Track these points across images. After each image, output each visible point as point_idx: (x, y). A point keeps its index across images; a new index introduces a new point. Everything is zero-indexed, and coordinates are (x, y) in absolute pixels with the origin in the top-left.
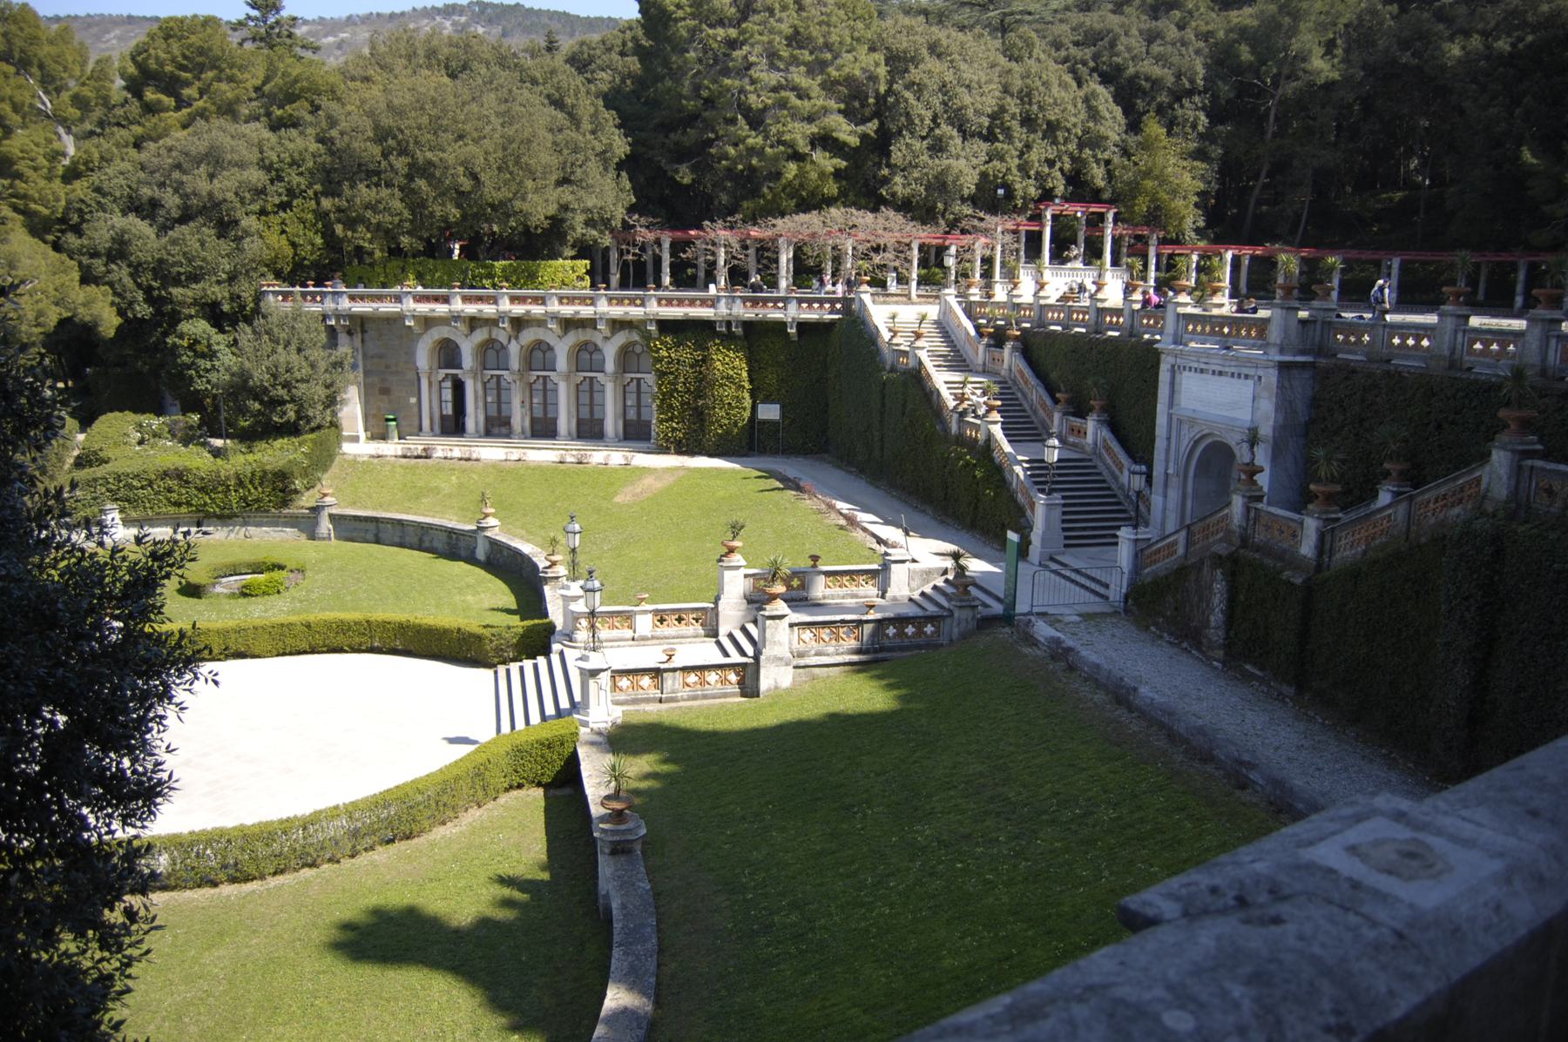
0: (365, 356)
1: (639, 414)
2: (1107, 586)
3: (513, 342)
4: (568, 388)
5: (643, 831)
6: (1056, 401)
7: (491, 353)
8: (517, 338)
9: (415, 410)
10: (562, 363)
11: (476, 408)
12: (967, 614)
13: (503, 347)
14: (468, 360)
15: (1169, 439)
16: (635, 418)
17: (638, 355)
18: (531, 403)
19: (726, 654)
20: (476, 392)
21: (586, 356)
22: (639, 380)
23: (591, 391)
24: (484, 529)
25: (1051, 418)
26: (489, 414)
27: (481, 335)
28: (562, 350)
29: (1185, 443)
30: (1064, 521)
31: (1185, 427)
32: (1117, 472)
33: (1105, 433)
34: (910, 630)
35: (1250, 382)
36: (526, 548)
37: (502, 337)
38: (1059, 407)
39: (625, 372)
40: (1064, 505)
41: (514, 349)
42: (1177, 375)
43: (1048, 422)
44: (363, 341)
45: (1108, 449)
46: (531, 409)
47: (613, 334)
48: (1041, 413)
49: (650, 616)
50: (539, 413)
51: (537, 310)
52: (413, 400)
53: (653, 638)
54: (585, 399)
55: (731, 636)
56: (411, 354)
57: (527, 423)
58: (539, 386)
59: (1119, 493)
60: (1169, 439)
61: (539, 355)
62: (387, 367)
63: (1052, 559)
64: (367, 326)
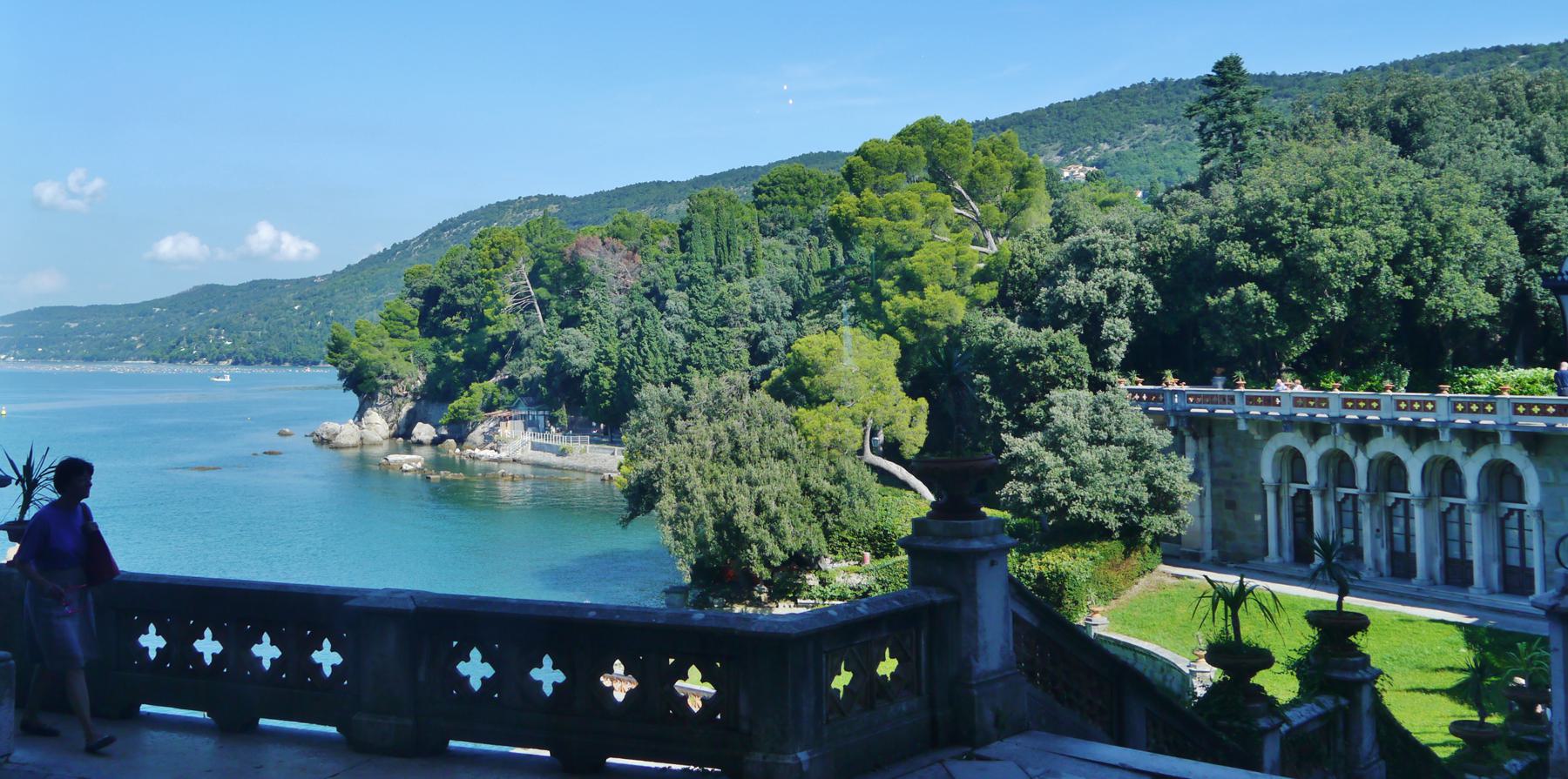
0: (1213, 464)
3: (1360, 454)
7: (1339, 467)
8: (1364, 451)
9: (1260, 528)
10: (1415, 485)
20: (1325, 513)
21: (1445, 476)
28: (1415, 463)
41: (1361, 463)
44: (1210, 446)
52: (1258, 518)
56: (1256, 465)
57: (1383, 555)
61: (1390, 473)
62: (1234, 477)
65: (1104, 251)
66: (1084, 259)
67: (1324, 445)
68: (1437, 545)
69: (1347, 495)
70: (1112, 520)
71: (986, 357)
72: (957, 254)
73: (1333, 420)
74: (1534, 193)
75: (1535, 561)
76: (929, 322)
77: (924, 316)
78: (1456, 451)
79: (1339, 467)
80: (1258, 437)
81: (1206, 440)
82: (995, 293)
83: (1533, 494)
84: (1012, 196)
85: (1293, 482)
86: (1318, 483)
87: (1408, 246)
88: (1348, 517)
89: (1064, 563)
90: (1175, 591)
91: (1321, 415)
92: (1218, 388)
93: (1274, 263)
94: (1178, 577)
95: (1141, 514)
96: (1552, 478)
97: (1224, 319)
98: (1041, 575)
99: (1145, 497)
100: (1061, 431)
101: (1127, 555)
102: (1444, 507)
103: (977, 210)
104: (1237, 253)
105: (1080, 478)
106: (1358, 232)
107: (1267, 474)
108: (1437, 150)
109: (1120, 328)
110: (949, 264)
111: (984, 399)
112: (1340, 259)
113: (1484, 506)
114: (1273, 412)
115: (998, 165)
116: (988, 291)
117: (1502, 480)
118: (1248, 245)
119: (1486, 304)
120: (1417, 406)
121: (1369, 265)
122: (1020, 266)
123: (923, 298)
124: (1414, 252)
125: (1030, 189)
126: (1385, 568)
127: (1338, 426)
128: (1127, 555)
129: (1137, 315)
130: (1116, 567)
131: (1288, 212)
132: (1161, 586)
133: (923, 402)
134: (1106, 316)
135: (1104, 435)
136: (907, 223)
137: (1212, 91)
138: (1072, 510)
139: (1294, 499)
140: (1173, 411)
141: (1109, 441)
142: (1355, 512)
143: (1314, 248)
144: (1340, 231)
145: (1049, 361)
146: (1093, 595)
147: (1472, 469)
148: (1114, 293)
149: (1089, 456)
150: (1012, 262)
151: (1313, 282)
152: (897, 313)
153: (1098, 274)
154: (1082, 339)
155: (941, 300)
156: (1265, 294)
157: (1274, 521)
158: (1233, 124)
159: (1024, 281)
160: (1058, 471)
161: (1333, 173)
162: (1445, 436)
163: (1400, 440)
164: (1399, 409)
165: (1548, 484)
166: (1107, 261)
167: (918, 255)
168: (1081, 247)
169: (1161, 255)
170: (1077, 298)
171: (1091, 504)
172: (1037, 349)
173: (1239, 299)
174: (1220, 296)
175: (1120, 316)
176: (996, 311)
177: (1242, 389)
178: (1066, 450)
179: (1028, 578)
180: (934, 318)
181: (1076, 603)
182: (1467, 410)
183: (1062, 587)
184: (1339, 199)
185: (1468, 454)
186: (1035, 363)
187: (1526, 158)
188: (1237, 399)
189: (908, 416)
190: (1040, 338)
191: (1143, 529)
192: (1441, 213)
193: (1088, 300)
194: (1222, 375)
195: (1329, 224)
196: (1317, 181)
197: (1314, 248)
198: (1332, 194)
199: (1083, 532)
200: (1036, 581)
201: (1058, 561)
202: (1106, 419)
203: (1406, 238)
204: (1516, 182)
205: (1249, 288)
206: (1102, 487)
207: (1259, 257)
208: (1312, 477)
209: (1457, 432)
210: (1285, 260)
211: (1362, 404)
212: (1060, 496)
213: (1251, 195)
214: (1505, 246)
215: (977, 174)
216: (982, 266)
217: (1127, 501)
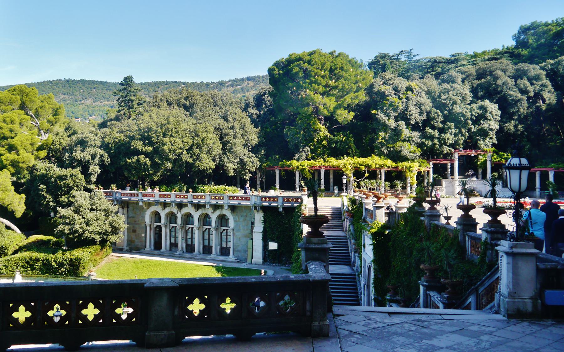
1: (227, 244)
3: (179, 213)
7: (172, 217)
8: (180, 212)
9: (144, 239)
10: (196, 222)
11: (166, 239)
16: (225, 246)
20: (166, 233)
21: (205, 220)
23: (209, 234)
26: (172, 242)
28: (196, 215)
39: (221, 227)
41: (179, 216)
44: (128, 211)
46: (187, 240)
51: (185, 201)
52: (143, 235)
56: (144, 217)
61: (188, 218)
62: (135, 221)
64: (130, 206)
65: (91, 141)
66: (82, 143)
67: (167, 210)
68: (202, 242)
69: (173, 226)
70: (98, 238)
71: (44, 179)
72: (32, 139)
73: (172, 202)
74: (225, 131)
75: (231, 245)
76: (20, 165)
77: (19, 162)
78: (209, 211)
79: (172, 217)
80: (146, 208)
81: (126, 209)
82: (46, 155)
83: (232, 224)
84: (51, 117)
85: (155, 222)
86: (164, 223)
87: (192, 145)
88: (173, 234)
89: (80, 254)
90: (118, 262)
91: (168, 200)
92: (128, 190)
93: (150, 149)
94: (118, 257)
95: (107, 235)
96: (237, 219)
97: (133, 168)
98: (71, 260)
99: (110, 229)
100: (80, 206)
101: (101, 250)
102: (204, 229)
103: (38, 123)
104: (138, 145)
105: (88, 223)
106: (178, 140)
107: (147, 220)
108: (199, 114)
109: (95, 169)
110: (29, 142)
111: (43, 194)
112: (172, 149)
113: (217, 229)
114: (152, 199)
115: (47, 106)
116: (43, 154)
117: (223, 220)
118: (142, 142)
119: (212, 165)
120: (199, 197)
121: (181, 151)
122: (55, 145)
123: (18, 155)
124: (194, 147)
125: (59, 116)
126: (185, 250)
127: (174, 204)
128: (101, 250)
129: (102, 165)
130: (98, 255)
131: (156, 131)
132: (112, 260)
133: (23, 196)
134: (90, 165)
135: (95, 208)
136: (13, 126)
137: (123, 87)
138: (85, 235)
139: (155, 228)
140: (116, 199)
141: (96, 210)
142: (176, 232)
143: (164, 144)
144: (172, 139)
145: (70, 180)
146: (91, 266)
147: (214, 217)
148: (93, 157)
149: (91, 215)
150: (53, 143)
151: (164, 156)
152: (8, 160)
153: (88, 149)
154: (82, 173)
155: (26, 156)
156: (147, 159)
157: (149, 237)
158: (130, 100)
159: (56, 151)
160: (80, 221)
161: (171, 120)
162: (208, 207)
163: (193, 208)
164: (194, 198)
165: (236, 221)
166: (91, 145)
167: (16, 138)
168: (82, 139)
169: (111, 144)
170: (81, 157)
171: (91, 233)
172: (66, 176)
173: (138, 160)
174: (132, 159)
175: (95, 165)
176: (45, 161)
177: (141, 191)
178: (82, 213)
179: (66, 261)
180: (23, 163)
181: (84, 268)
182: (215, 198)
183: (79, 263)
184: (172, 129)
185: (213, 212)
186: (65, 181)
187: (223, 120)
188: (139, 195)
189: (18, 201)
190: (67, 172)
191: (108, 241)
192: (202, 135)
193: (84, 159)
194: (129, 186)
195: (169, 137)
196: (166, 122)
197: (164, 144)
198: (170, 127)
199: (87, 243)
200: (70, 261)
201: (78, 254)
202: (96, 202)
203: (192, 143)
204: (221, 127)
205: (142, 157)
206: (95, 227)
207: (145, 146)
208: (163, 220)
209: (211, 206)
210: (154, 148)
211: (240, 198)
212: (80, 230)
213: (144, 125)
214: (218, 148)
215: (39, 109)
216: (40, 144)
217: (104, 231)
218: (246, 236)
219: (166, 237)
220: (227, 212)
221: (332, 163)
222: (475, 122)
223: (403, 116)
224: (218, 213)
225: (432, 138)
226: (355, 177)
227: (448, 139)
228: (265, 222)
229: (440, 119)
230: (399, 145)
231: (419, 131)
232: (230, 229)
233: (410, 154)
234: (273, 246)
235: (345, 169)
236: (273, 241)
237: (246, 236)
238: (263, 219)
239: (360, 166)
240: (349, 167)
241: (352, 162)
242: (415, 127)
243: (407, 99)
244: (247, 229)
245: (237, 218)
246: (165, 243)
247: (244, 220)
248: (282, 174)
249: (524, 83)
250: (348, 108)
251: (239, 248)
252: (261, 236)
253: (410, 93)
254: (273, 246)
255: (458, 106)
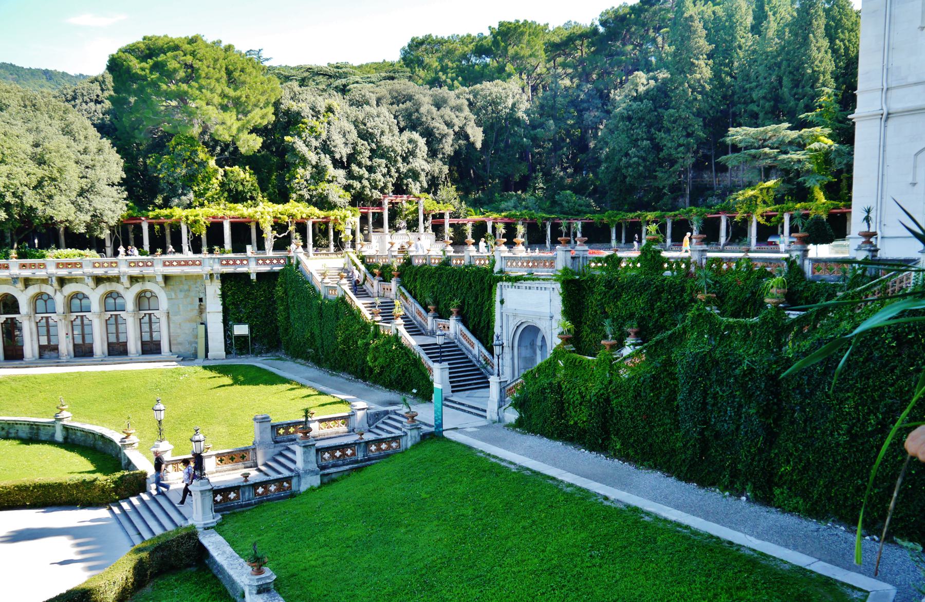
2: (485, 411)
3: (58, 293)
4: (101, 323)
5: (274, 577)
6: (427, 311)
8: (61, 291)
10: (95, 306)
12: (415, 432)
13: (50, 298)
14: (24, 307)
15: (502, 327)
17: (149, 299)
18: (73, 334)
19: (279, 473)
20: (31, 329)
21: (111, 300)
22: (150, 315)
24: (61, 420)
25: (426, 320)
27: (33, 290)
28: (95, 295)
29: (512, 327)
30: (450, 378)
31: (511, 319)
32: (471, 348)
33: (461, 326)
34: (384, 446)
35: (547, 292)
36: (98, 429)
37: (48, 289)
38: (430, 314)
40: (450, 369)
41: (59, 300)
42: (504, 290)
43: (424, 323)
45: (464, 336)
46: (73, 339)
47: (131, 285)
48: (419, 318)
49: (214, 457)
50: (79, 341)
53: (217, 472)
54: (112, 329)
55: (266, 465)
58: (78, 322)
59: (474, 360)
60: (502, 327)
63: (446, 400)
96: (174, 296)
124: (45, 183)
127: (54, 279)
218: (191, 321)
219: (31, 333)
220: (156, 288)
221: (240, 212)
222: (405, 159)
223: (326, 148)
224: (137, 288)
225: (360, 178)
226: (275, 232)
227: (380, 181)
228: (224, 296)
229: (368, 154)
230: (323, 186)
231: (343, 167)
232: (160, 314)
233: (340, 200)
234: (241, 330)
235: (263, 220)
236: (240, 322)
237: (191, 321)
238: (220, 293)
239: (282, 216)
240: (269, 218)
241: (271, 210)
242: (337, 164)
243: (329, 123)
244: (192, 310)
245: (173, 294)
246: (30, 348)
247: (186, 297)
248: (156, 230)
249: (446, 111)
250: (255, 130)
251: (180, 340)
252: (220, 317)
253: (331, 115)
254: (241, 330)
255: (385, 137)
